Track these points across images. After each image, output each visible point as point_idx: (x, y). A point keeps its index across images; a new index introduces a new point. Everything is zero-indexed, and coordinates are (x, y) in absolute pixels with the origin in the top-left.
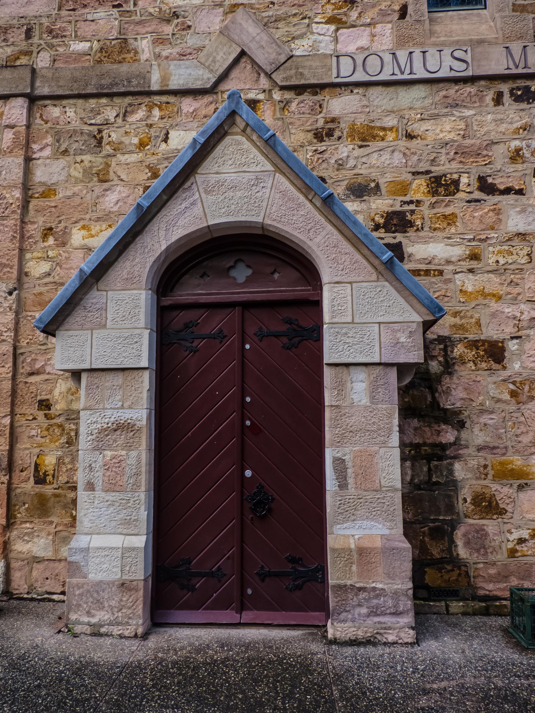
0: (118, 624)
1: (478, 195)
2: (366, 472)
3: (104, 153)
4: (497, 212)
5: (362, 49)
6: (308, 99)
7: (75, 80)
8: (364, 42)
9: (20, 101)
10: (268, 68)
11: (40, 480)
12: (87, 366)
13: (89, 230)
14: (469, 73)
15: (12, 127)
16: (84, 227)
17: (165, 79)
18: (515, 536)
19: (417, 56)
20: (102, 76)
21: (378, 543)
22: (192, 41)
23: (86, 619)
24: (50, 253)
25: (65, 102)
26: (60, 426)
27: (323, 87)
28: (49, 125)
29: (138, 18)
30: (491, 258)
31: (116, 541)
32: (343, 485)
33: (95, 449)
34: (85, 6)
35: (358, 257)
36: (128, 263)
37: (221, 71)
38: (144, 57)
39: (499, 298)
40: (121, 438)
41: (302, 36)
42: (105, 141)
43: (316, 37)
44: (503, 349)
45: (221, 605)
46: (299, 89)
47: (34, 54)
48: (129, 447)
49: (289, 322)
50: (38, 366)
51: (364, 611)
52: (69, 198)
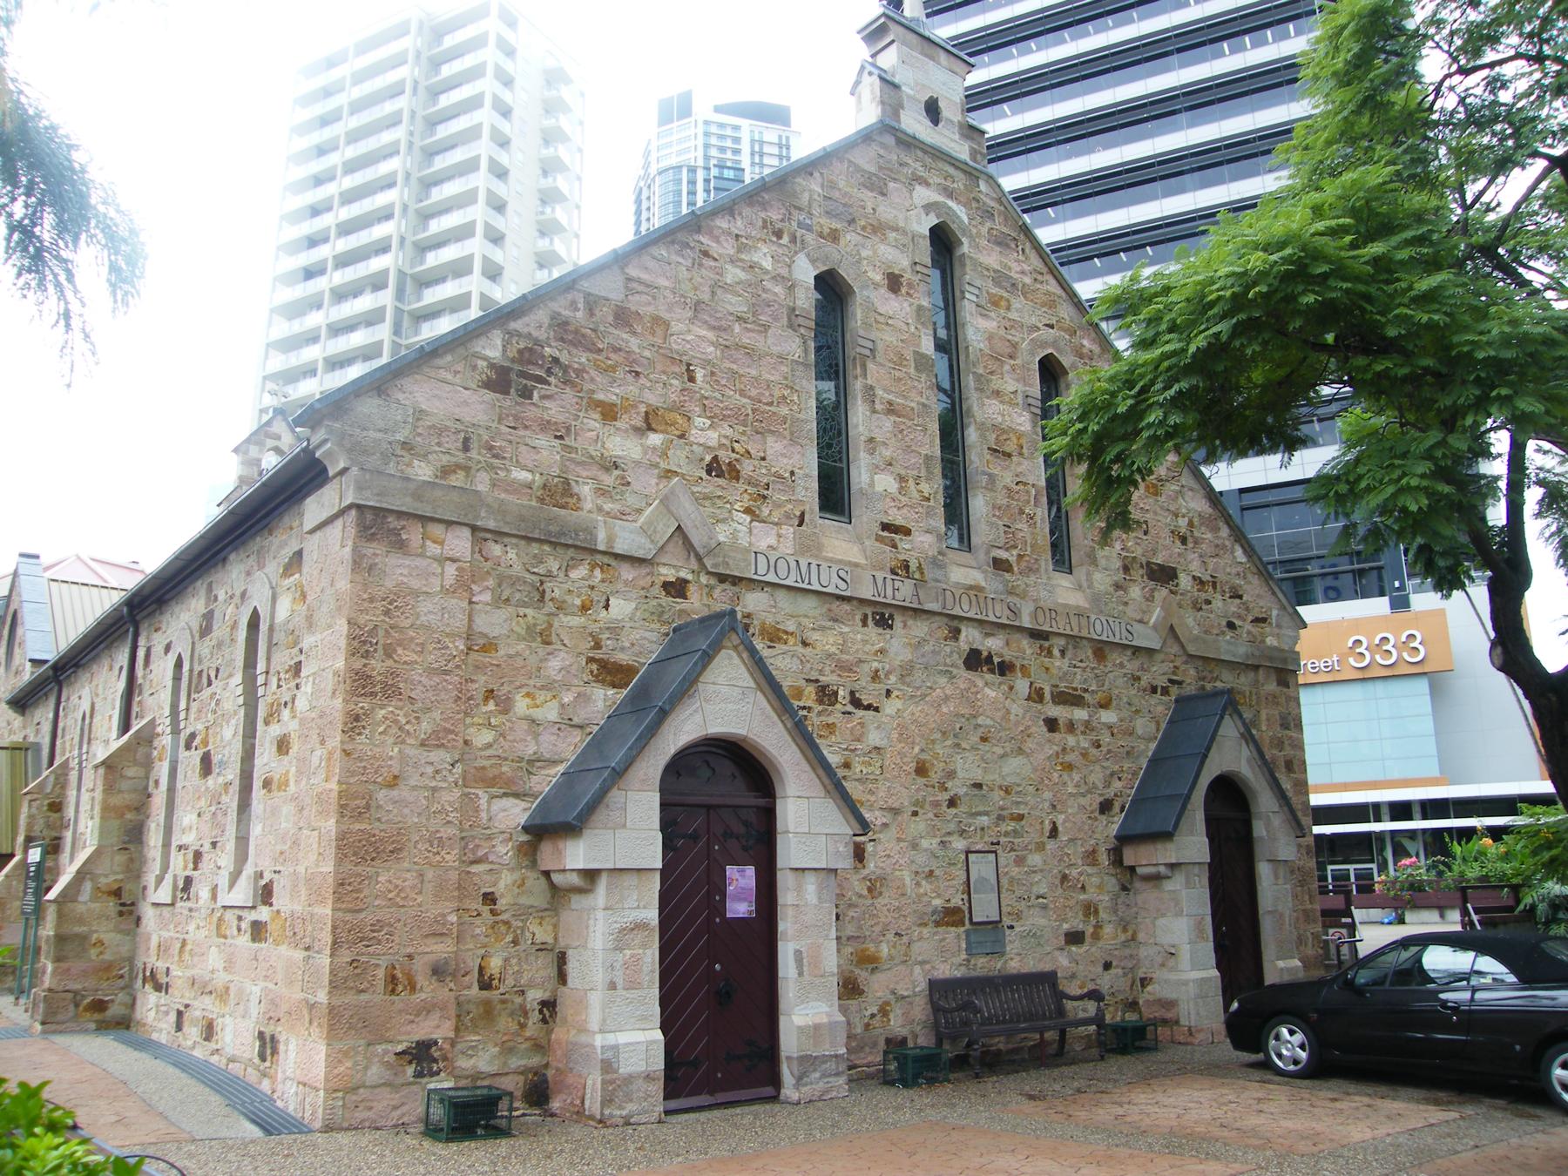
0: (646, 1112)
1: (850, 708)
4: (862, 725)
7: (522, 519)
8: (772, 541)
10: (701, 551)
11: (485, 985)
13: (534, 699)
14: (848, 593)
15: (454, 560)
16: (528, 695)
17: (610, 539)
18: (868, 1013)
20: (550, 520)
22: (632, 500)
25: (506, 540)
26: (506, 923)
27: (741, 579)
29: (579, 457)
31: (639, 1036)
33: (616, 949)
34: (526, 427)
35: (813, 776)
36: (644, 764)
38: (588, 505)
40: (639, 937)
41: (724, 521)
42: (547, 597)
46: (722, 578)
48: (644, 946)
50: (480, 853)
51: (817, 1075)
52: (510, 657)
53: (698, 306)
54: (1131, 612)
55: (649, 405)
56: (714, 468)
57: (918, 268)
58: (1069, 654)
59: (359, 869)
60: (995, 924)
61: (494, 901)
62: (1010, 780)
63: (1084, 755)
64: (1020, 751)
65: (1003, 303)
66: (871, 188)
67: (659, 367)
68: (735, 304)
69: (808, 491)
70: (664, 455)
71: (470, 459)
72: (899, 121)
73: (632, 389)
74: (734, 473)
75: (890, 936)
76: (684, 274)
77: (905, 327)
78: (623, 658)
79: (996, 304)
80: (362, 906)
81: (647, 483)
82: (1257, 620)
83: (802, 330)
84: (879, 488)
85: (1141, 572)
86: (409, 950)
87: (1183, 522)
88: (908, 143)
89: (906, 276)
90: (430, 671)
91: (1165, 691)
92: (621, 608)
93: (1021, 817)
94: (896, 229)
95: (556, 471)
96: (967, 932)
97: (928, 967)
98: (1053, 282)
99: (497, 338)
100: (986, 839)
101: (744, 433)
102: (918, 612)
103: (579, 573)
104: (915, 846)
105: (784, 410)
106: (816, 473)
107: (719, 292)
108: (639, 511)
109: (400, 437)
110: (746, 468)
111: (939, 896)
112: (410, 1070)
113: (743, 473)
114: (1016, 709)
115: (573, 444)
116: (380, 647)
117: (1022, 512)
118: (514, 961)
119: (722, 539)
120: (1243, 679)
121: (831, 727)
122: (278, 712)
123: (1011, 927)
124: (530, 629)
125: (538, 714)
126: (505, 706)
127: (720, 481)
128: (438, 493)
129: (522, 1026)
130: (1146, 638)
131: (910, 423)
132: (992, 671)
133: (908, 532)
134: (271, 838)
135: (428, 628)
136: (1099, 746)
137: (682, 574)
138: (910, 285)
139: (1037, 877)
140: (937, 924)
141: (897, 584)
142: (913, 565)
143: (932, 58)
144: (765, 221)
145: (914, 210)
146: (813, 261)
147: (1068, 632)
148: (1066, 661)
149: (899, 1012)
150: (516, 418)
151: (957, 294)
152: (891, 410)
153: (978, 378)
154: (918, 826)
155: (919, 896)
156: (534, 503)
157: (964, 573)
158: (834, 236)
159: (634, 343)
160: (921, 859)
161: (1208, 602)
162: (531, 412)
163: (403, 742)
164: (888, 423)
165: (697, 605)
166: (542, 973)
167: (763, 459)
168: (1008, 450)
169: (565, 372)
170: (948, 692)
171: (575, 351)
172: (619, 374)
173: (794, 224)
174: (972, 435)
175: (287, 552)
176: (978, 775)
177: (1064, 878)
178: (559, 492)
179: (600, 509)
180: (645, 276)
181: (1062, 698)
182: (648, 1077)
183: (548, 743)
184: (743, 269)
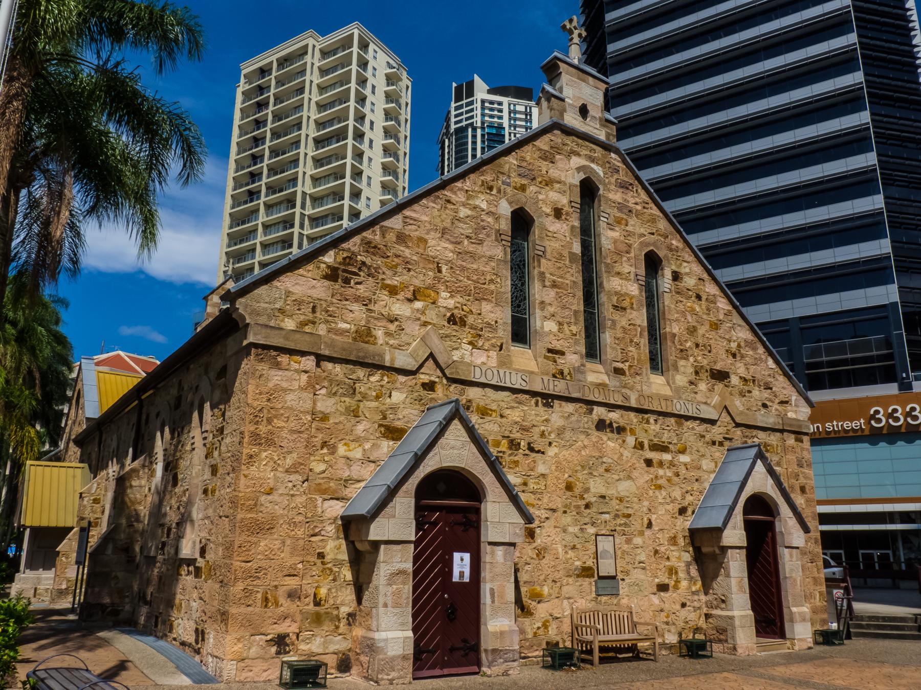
1: (527, 452)
3: (356, 398)
4: (534, 462)
5: (484, 363)
6: (460, 387)
8: (484, 359)
9: (313, 358)
10: (443, 366)
11: (317, 603)
12: (385, 538)
15: (306, 372)
16: (345, 444)
17: (392, 360)
18: (536, 626)
19: (508, 374)
20: (359, 350)
21: (507, 629)
22: (404, 338)
23: (386, 677)
24: (326, 458)
26: (330, 569)
28: (326, 374)
30: (531, 486)
31: (399, 634)
34: (347, 300)
37: (421, 362)
38: (380, 341)
39: (533, 506)
40: (400, 578)
41: (457, 349)
43: (463, 351)
44: (534, 532)
45: (432, 667)
47: (317, 325)
48: (404, 583)
49: (465, 517)
50: (317, 530)
52: (336, 424)
53: (444, 231)
54: (699, 397)
55: (415, 286)
57: (573, 204)
58: (660, 422)
59: (250, 539)
60: (613, 578)
61: (323, 557)
62: (622, 494)
63: (669, 480)
64: (629, 477)
65: (623, 222)
66: (545, 158)
67: (421, 265)
68: (465, 229)
69: (505, 332)
70: (423, 313)
71: (316, 317)
72: (563, 120)
73: (406, 278)
74: (463, 323)
75: (549, 581)
76: (436, 213)
77: (563, 238)
78: (399, 424)
80: (250, 559)
81: (413, 329)
82: (782, 403)
83: (504, 242)
84: (546, 329)
85: (706, 374)
86: (276, 583)
87: (734, 345)
88: (568, 132)
89: (565, 209)
90: (292, 432)
91: (721, 444)
92: (398, 397)
93: (629, 516)
94: (559, 182)
95: (363, 323)
96: (595, 581)
97: (572, 601)
98: (654, 207)
100: (608, 527)
101: (468, 300)
104: (565, 531)
105: (492, 287)
106: (510, 321)
107: (456, 222)
108: (409, 344)
109: (277, 306)
110: (470, 320)
111: (579, 560)
112: (274, 649)
113: (468, 322)
114: (626, 454)
115: (372, 308)
116: (265, 419)
117: (631, 341)
118: (333, 590)
119: (455, 358)
120: (772, 437)
121: (516, 463)
122: (212, 452)
123: (623, 580)
124: (347, 408)
125: (351, 455)
126: (333, 450)
127: (455, 327)
128: (298, 336)
129: (337, 627)
130: (709, 413)
131: (565, 292)
132: (612, 432)
133: (563, 353)
134: (206, 521)
135: (291, 408)
136: (678, 475)
137: (433, 378)
138: (567, 214)
139: (639, 551)
140: (578, 576)
141: (556, 383)
142: (566, 372)
143: (584, 81)
144: (483, 181)
145: (569, 170)
146: (510, 203)
147: (659, 409)
148: (658, 426)
149: (555, 627)
150: (341, 295)
151: (596, 217)
152: (554, 285)
153: (607, 265)
154: (567, 519)
155: (567, 560)
156: (350, 341)
157: (596, 374)
158: (523, 188)
159: (407, 252)
160: (568, 538)
161: (750, 392)
162: (349, 292)
163: (276, 470)
164: (552, 293)
165: (441, 395)
166: (350, 597)
167: (480, 314)
168: (624, 306)
169: (369, 269)
170: (586, 443)
171: (374, 258)
172: (399, 269)
173: (500, 182)
174: (603, 298)
175: (218, 366)
176: (603, 491)
177: (656, 552)
178: (364, 335)
179: (387, 344)
180: (413, 215)
181: (655, 447)
182: (404, 658)
183: (356, 471)
184: (470, 209)
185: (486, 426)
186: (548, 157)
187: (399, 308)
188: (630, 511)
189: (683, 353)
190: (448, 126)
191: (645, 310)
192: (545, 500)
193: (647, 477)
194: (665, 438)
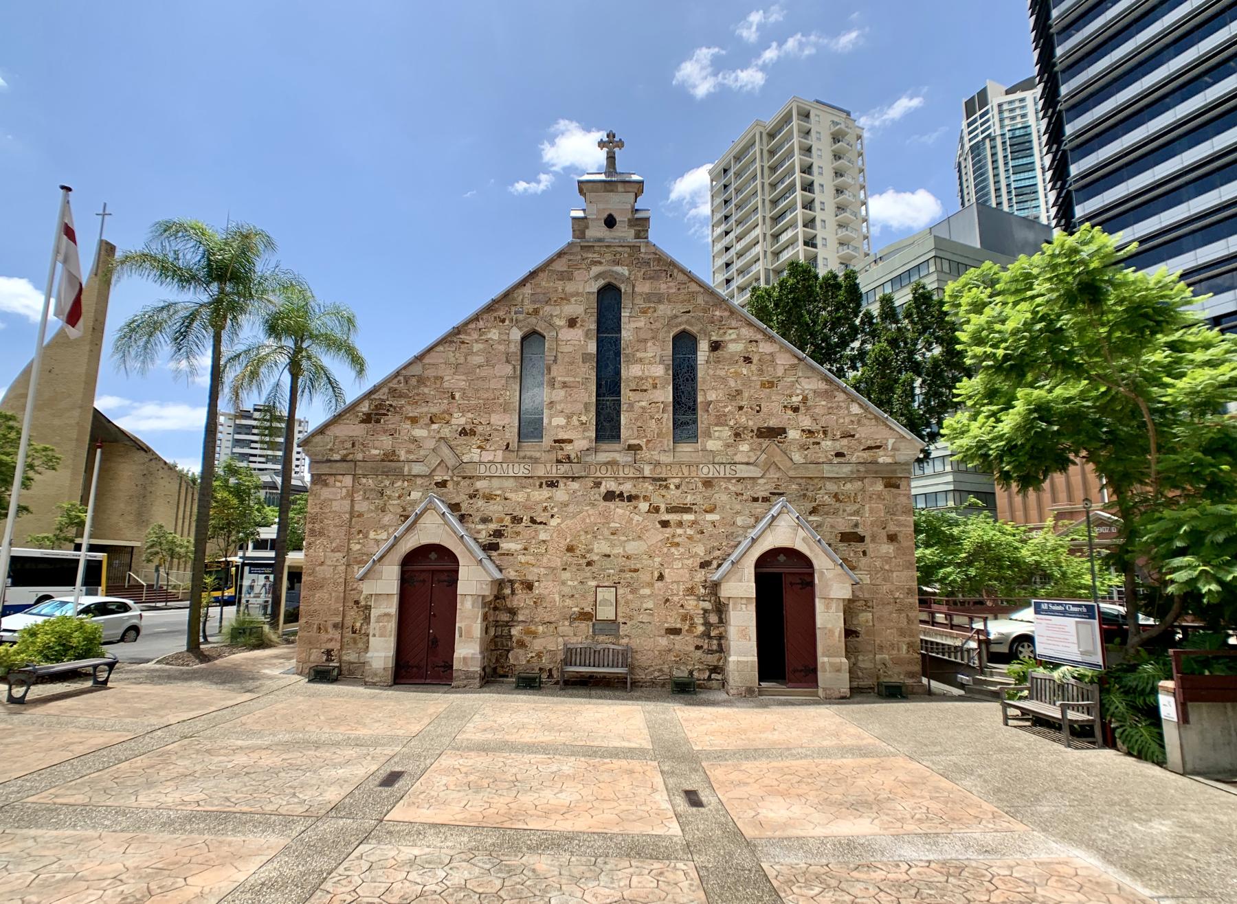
2: (469, 632)
8: (491, 458)
11: (354, 632)
17: (410, 470)
22: (422, 452)
32: (461, 636)
40: (386, 618)
56: (464, 432)
60: (614, 621)
68: (479, 359)
73: (425, 410)
74: (473, 433)
79: (645, 312)
91: (765, 500)
92: (415, 495)
93: (636, 571)
99: (366, 403)
102: (574, 479)
103: (399, 483)
104: (564, 583)
110: (480, 429)
112: (325, 658)
121: (518, 534)
124: (377, 508)
125: (378, 537)
126: (366, 537)
133: (570, 441)
138: (583, 321)
142: (572, 456)
146: (520, 329)
152: (565, 385)
153: (627, 356)
155: (564, 607)
158: (536, 311)
159: (426, 390)
160: (566, 590)
164: (562, 393)
177: (667, 600)
180: (431, 361)
181: (671, 510)
185: (491, 508)
186: (566, 276)
187: (419, 432)
188: (639, 566)
189: (721, 420)
190: (963, 146)
191: (670, 388)
192: (545, 560)
193: (660, 537)
194: (689, 499)
